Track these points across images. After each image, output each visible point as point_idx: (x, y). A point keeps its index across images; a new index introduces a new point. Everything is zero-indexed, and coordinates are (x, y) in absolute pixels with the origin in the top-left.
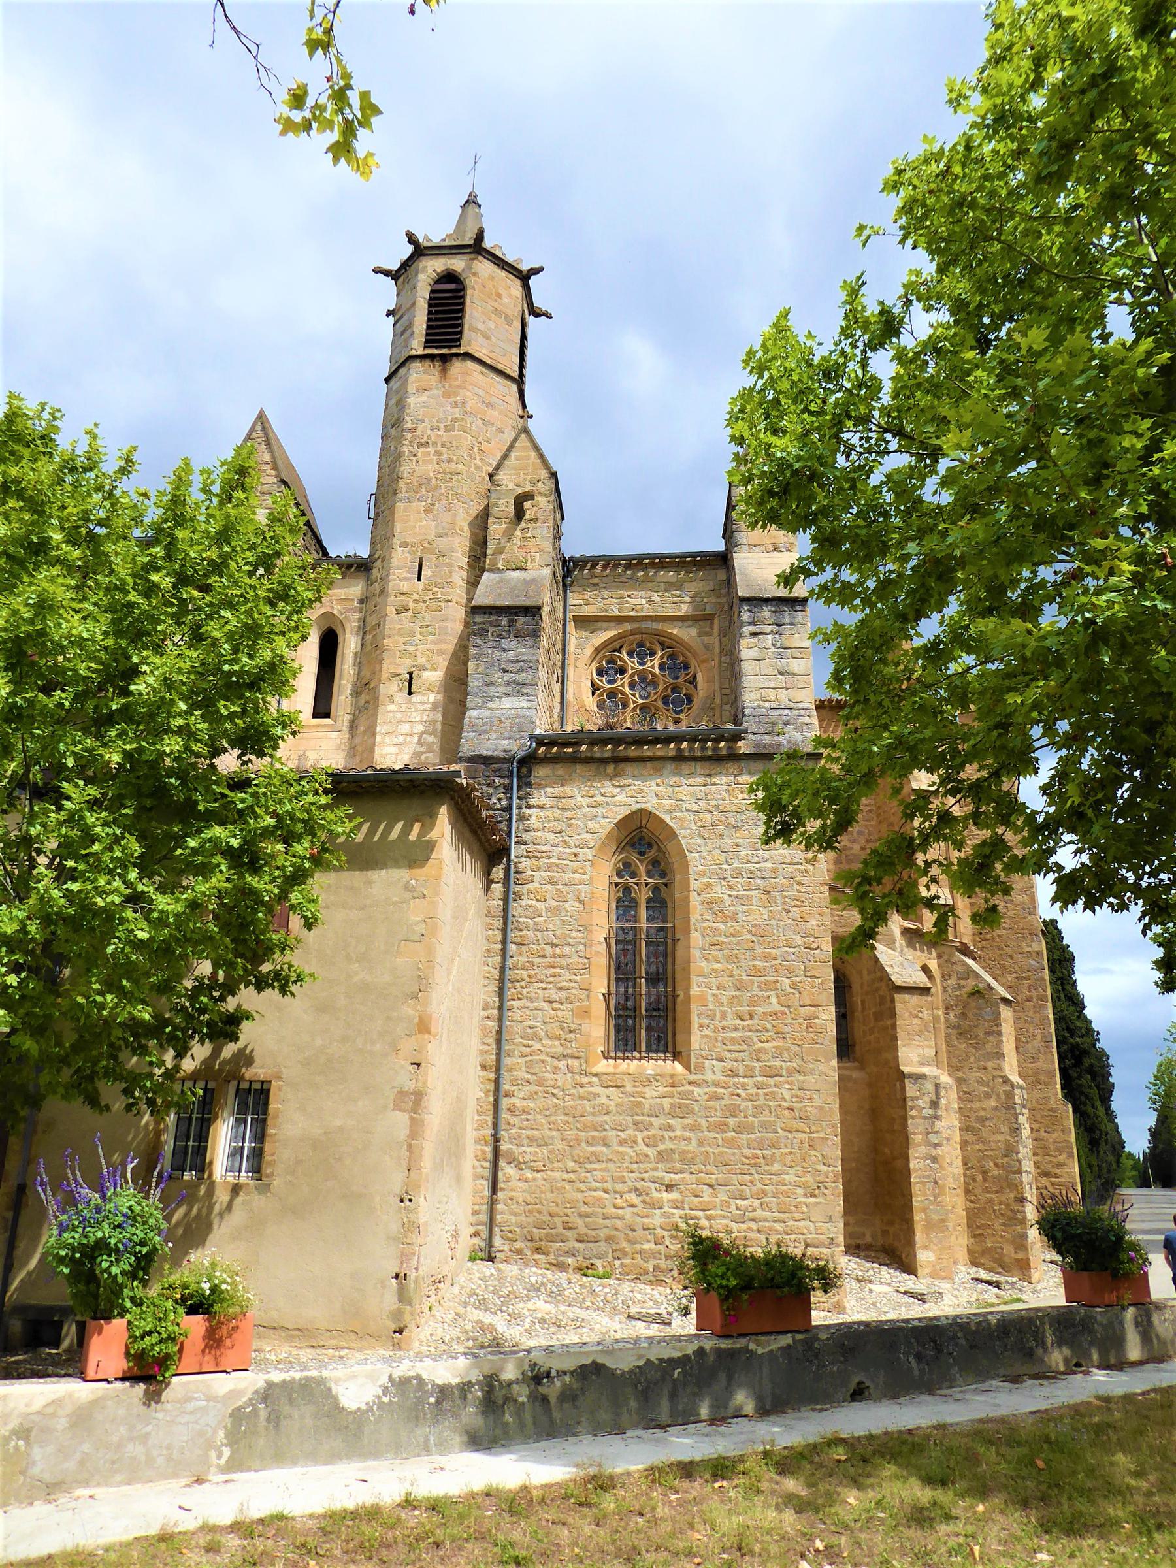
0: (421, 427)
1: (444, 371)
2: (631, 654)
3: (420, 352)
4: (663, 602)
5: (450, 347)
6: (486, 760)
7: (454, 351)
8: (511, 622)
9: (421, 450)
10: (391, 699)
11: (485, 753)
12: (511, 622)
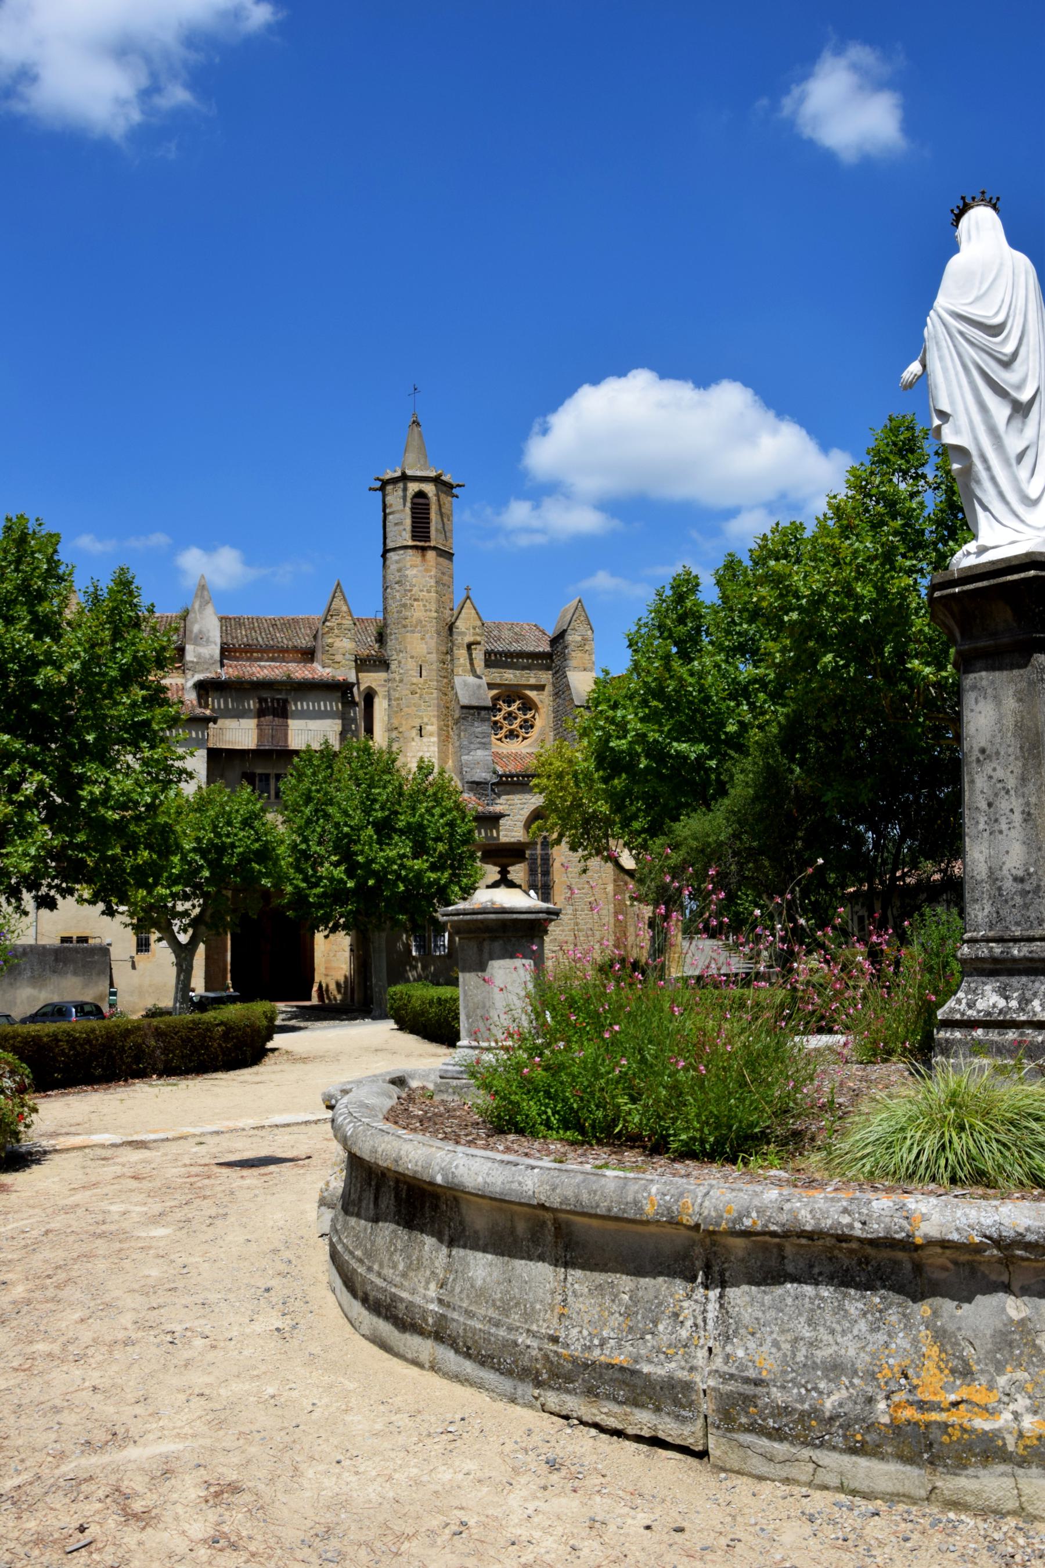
0: (415, 589)
1: (423, 556)
2: (504, 702)
3: (410, 543)
4: (522, 676)
5: (425, 541)
6: (478, 783)
7: (427, 544)
8: (479, 714)
9: (416, 603)
10: (413, 739)
11: (478, 780)
12: (479, 714)
